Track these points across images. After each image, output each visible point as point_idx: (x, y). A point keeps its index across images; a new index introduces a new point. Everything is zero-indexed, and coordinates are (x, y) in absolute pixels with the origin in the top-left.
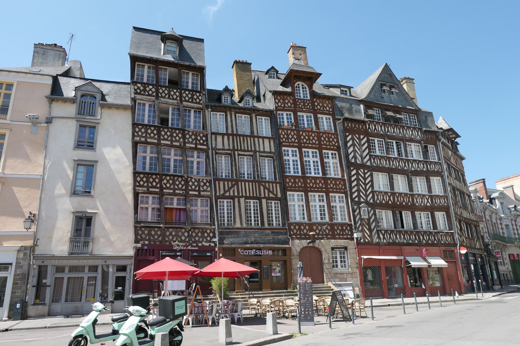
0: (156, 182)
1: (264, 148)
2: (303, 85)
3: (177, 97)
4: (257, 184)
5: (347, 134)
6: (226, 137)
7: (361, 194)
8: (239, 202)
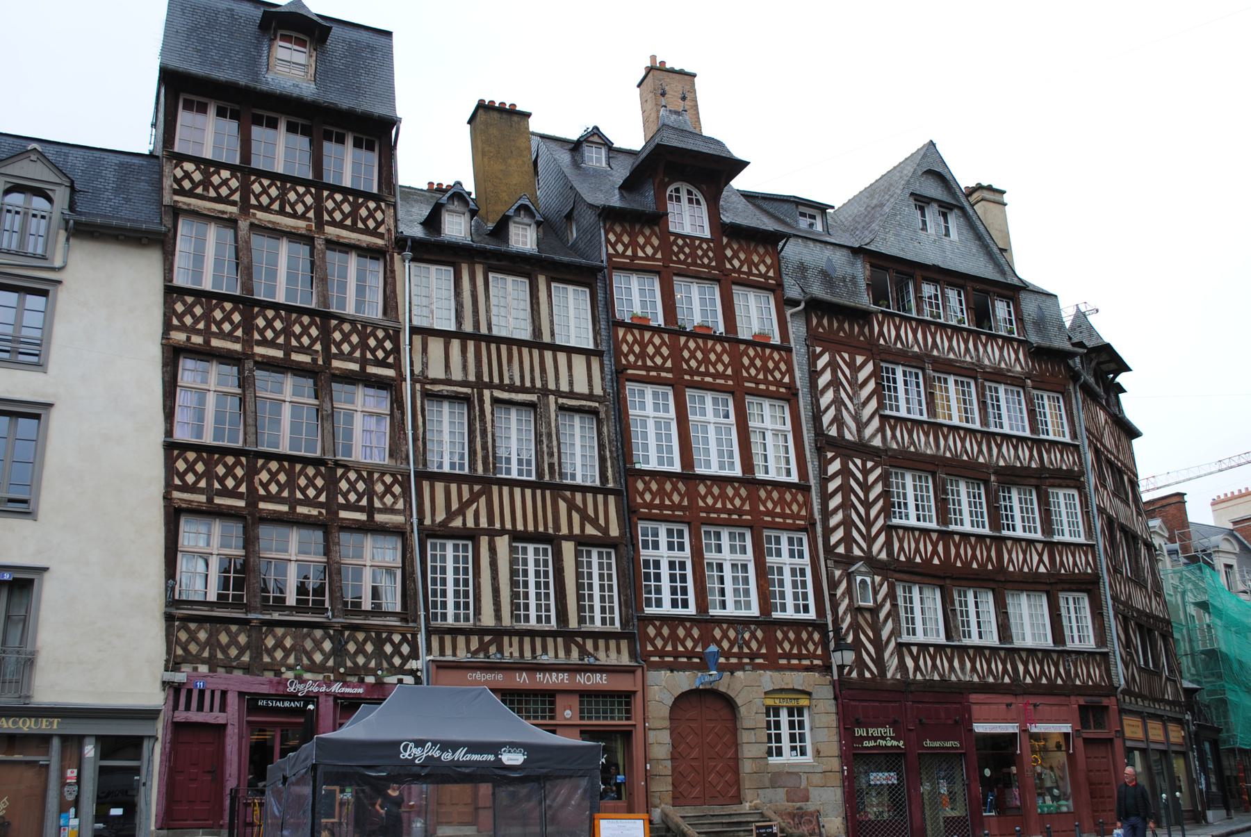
0: (235, 477)
1: (571, 383)
2: (689, 193)
3: (308, 209)
4: (548, 493)
5: (818, 350)
6: (455, 344)
7: (855, 534)
8: (493, 550)
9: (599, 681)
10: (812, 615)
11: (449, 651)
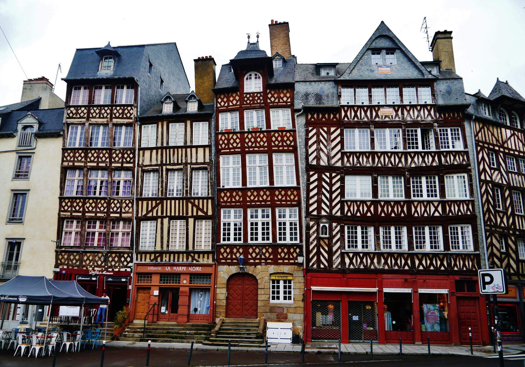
1: (197, 159)
2: (256, 75)
4: (185, 201)
7: (323, 206)
8: (162, 223)
9: (198, 269)
10: (298, 242)
11: (143, 260)
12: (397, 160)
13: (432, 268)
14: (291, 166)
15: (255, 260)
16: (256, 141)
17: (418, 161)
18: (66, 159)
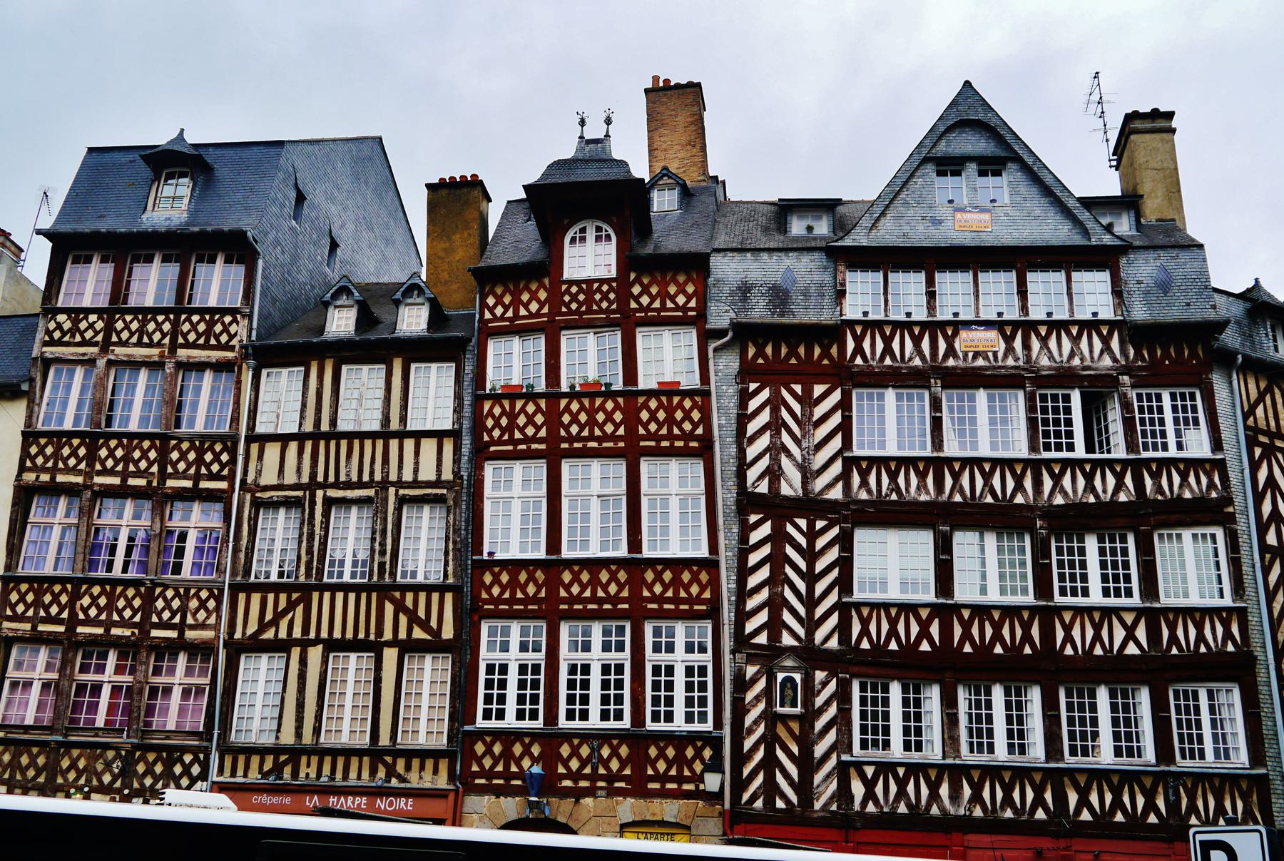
1: (416, 471)
2: (599, 229)
4: (374, 595)
7: (787, 617)
8: (303, 662)
10: (708, 726)
11: (240, 772)
12: (1010, 484)
13: (1119, 817)
14: (695, 497)
15: (576, 782)
16: (592, 422)
17: (1074, 486)
18: (33, 462)
